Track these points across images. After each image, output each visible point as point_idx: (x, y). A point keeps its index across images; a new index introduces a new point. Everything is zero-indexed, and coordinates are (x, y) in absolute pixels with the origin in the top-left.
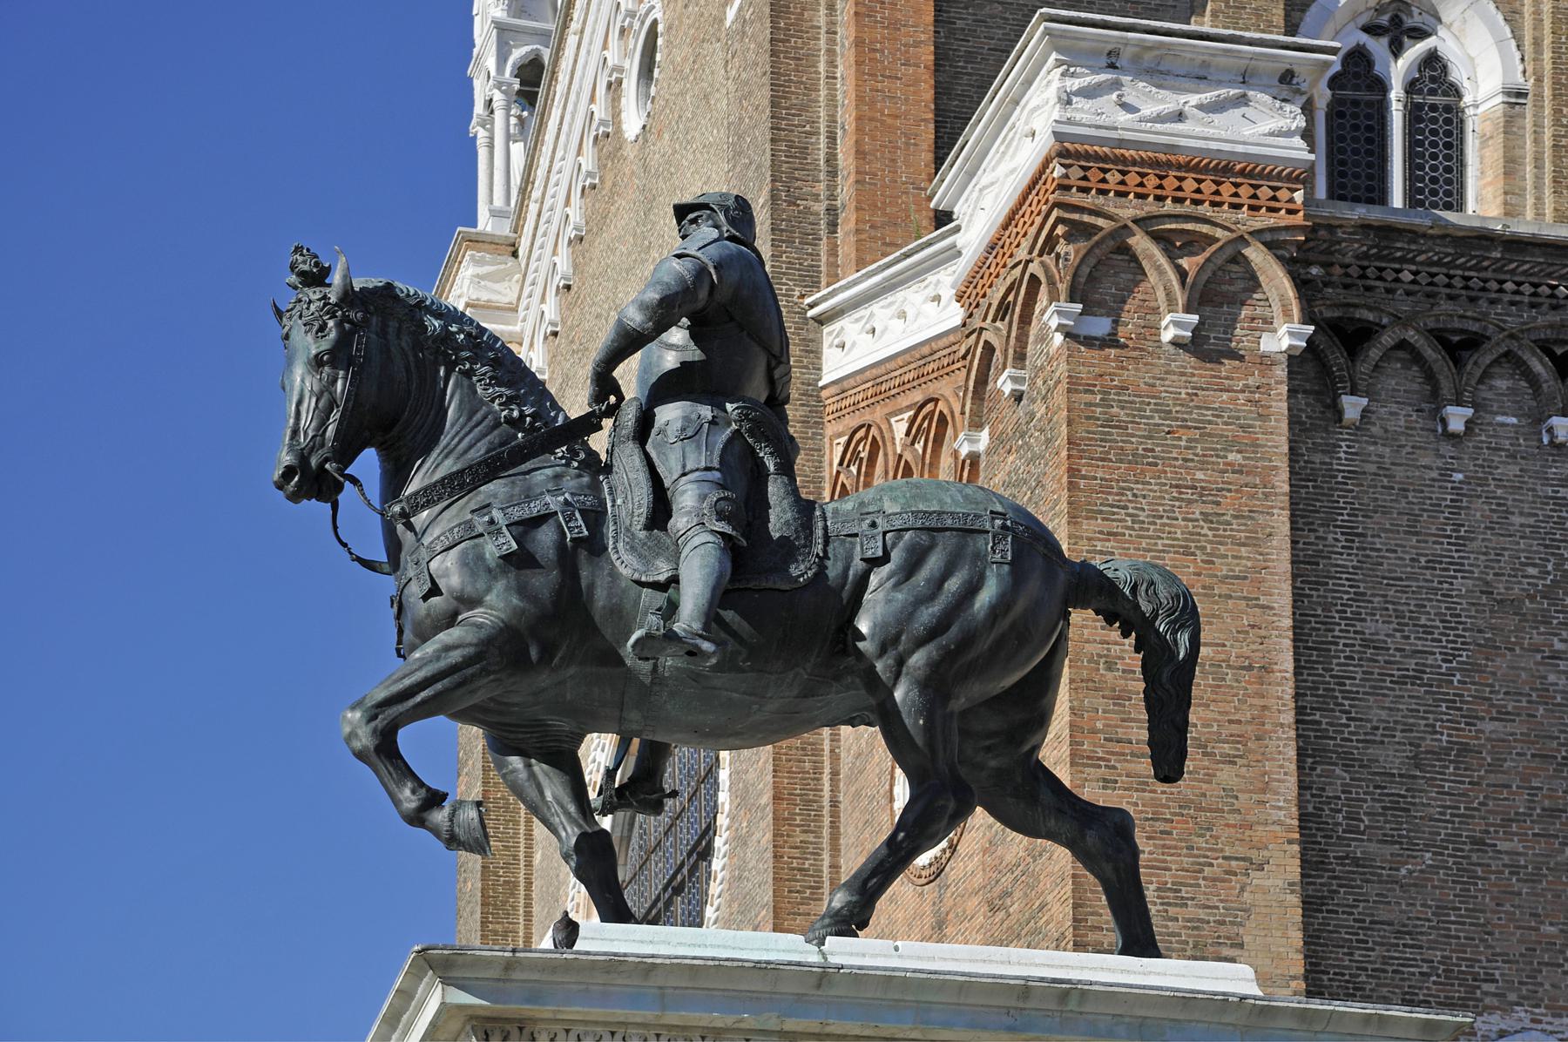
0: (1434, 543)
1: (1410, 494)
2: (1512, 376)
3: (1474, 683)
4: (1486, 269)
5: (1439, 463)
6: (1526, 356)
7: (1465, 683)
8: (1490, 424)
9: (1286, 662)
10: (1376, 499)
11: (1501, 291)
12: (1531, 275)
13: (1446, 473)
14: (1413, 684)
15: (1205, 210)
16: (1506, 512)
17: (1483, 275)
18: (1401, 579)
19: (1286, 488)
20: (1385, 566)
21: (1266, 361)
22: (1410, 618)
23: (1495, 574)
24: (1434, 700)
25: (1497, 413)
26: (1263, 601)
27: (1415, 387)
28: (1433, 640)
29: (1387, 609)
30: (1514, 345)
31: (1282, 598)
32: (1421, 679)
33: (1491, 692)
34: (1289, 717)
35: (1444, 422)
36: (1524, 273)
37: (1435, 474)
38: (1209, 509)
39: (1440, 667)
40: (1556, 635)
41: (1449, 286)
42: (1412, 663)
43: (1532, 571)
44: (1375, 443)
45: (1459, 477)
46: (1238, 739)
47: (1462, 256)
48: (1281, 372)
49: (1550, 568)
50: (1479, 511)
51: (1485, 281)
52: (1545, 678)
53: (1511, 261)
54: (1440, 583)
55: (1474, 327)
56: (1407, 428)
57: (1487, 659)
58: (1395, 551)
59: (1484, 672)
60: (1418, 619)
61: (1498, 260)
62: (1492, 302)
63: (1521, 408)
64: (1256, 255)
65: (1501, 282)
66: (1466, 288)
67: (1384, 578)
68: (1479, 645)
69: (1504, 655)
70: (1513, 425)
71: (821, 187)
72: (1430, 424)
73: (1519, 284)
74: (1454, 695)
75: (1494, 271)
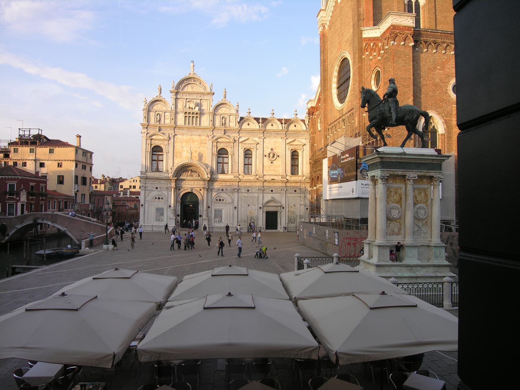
9: (412, 78)
15: (405, 31)
19: (412, 60)
21: (410, 46)
26: (410, 71)
31: (412, 71)
34: (412, 83)
38: (405, 62)
46: (408, 86)
48: (411, 47)
64: (409, 36)
71: (362, 16)
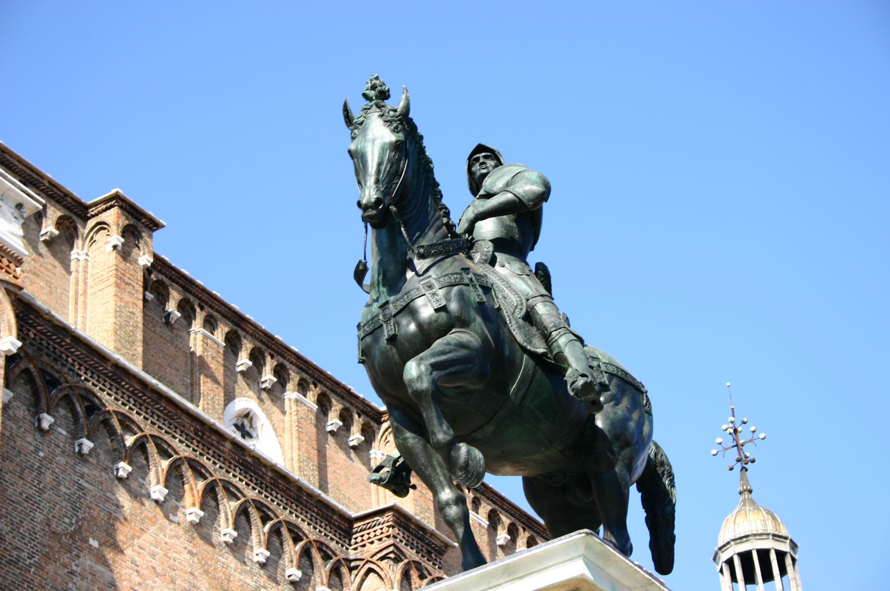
0: (30, 487)
1: (22, 456)
2: (65, 409)
3: (39, 576)
4: (62, 346)
5: (34, 443)
6: (75, 400)
7: (35, 574)
8: (56, 431)
10: (8, 452)
11: (66, 361)
12: (79, 358)
13: (37, 450)
14: (14, 566)
16: (59, 482)
17: (61, 349)
18: (14, 502)
20: (8, 492)
22: (17, 527)
23: (53, 516)
24: (23, 579)
25: (59, 426)
27: (28, 396)
28: (25, 544)
29: (7, 517)
30: (71, 393)
32: (18, 564)
33: (46, 584)
35: (39, 420)
36: (77, 356)
37: (32, 448)
39: (26, 560)
40: (74, 561)
41: (47, 348)
42: (15, 553)
43: (67, 520)
44: (10, 420)
45: (41, 454)
47: (55, 335)
49: (74, 521)
50: (48, 478)
51: (62, 353)
52: (67, 584)
53: (74, 348)
54: (30, 511)
55: (57, 375)
56: (24, 418)
57: (46, 564)
58: (13, 485)
59: (43, 570)
60: (19, 529)
61: (68, 344)
62: (63, 365)
63: (68, 428)
65: (68, 357)
66: (54, 352)
67: (8, 499)
68: (42, 554)
69: (52, 564)
70: (65, 436)
72: (32, 420)
73: (74, 361)
74: (31, 580)
75: (66, 349)
